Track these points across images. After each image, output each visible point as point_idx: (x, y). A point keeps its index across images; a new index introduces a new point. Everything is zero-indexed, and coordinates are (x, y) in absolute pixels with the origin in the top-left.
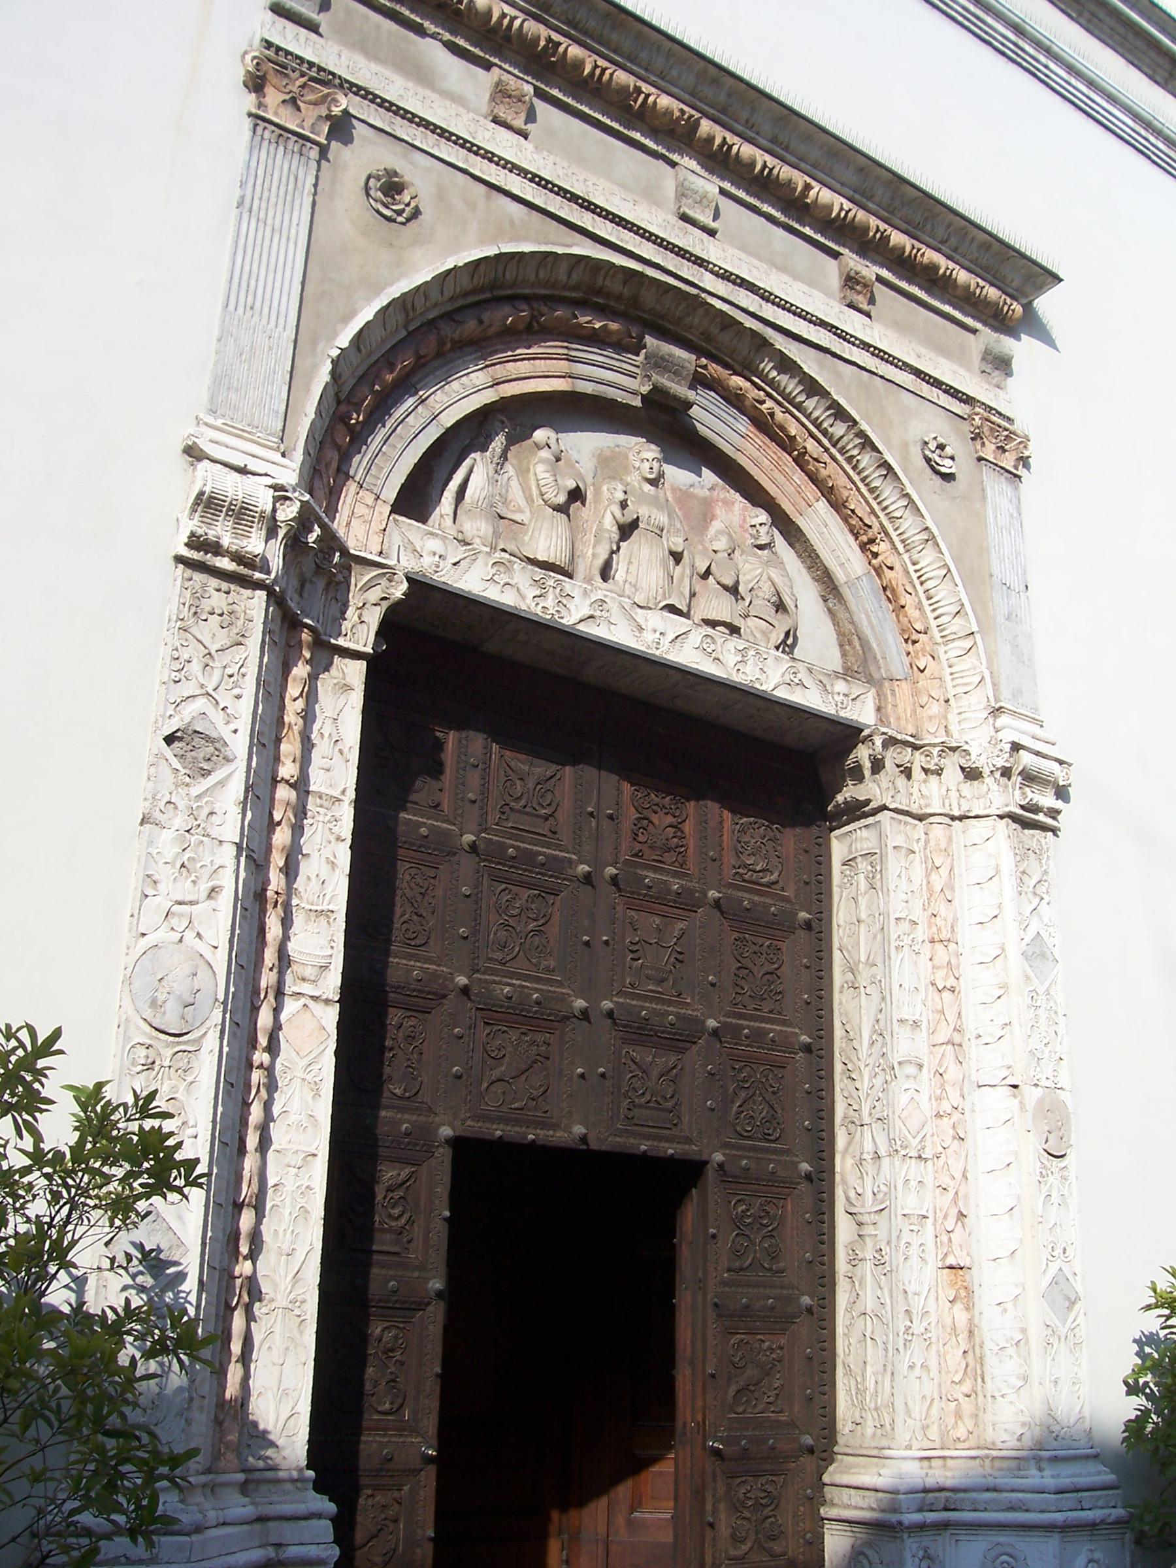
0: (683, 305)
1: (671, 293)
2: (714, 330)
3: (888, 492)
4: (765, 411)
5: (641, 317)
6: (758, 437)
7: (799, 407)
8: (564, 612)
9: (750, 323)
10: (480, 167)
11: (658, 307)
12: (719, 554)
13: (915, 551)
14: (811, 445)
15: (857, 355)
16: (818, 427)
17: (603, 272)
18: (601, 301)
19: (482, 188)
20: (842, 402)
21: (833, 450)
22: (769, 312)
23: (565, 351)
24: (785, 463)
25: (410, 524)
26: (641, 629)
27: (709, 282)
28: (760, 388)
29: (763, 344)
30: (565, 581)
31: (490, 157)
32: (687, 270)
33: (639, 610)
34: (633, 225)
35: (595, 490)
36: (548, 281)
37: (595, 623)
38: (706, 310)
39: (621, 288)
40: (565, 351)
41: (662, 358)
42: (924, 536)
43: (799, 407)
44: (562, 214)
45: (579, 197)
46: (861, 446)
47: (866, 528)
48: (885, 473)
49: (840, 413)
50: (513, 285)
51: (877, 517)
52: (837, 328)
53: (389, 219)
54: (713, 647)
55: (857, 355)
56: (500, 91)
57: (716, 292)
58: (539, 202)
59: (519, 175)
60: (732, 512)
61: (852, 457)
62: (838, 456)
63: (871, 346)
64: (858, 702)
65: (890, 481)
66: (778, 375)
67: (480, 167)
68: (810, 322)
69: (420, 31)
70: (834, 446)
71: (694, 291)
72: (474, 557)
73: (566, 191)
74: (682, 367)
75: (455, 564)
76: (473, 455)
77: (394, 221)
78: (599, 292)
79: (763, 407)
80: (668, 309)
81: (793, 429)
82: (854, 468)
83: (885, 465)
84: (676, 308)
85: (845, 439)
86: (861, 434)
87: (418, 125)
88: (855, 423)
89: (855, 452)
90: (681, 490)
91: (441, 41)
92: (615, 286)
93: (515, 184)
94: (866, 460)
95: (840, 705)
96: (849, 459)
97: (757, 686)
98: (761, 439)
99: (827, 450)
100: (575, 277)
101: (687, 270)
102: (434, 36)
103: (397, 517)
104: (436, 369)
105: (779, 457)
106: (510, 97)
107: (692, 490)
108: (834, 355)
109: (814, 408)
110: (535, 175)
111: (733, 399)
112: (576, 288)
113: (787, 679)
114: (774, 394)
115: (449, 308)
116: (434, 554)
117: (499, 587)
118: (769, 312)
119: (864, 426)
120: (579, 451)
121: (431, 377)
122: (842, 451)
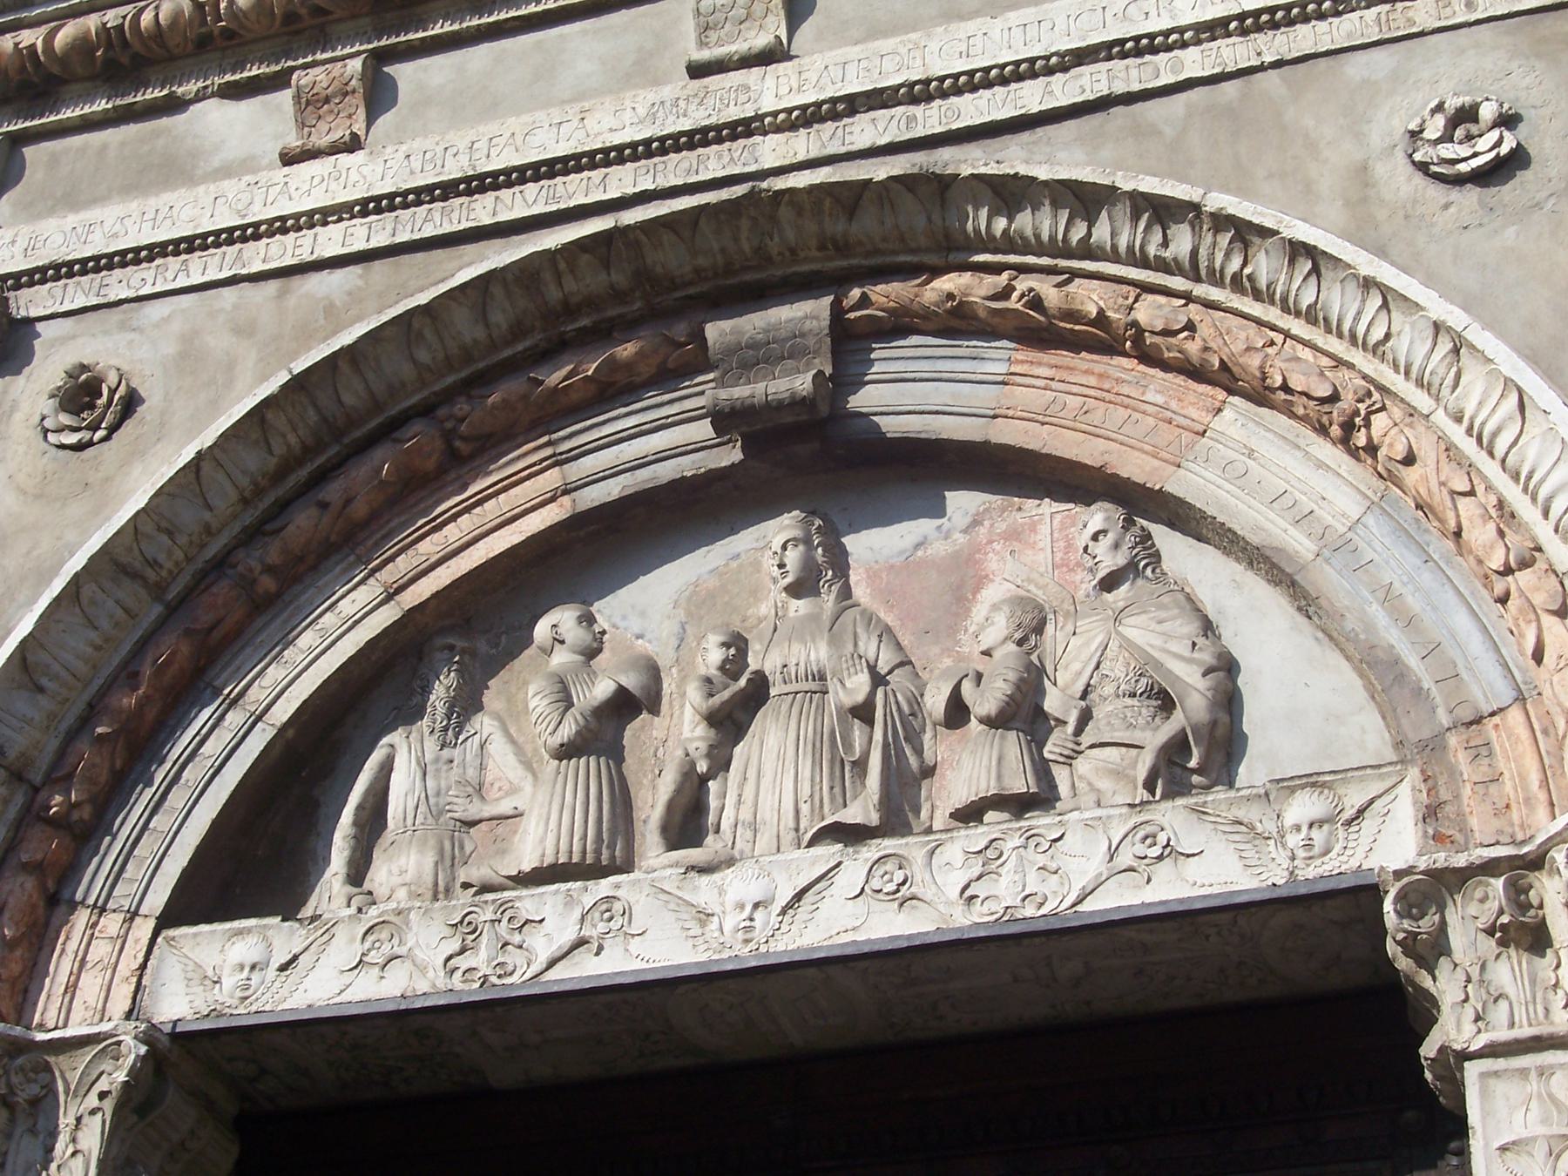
0: (745, 224)
1: (703, 222)
2: (838, 227)
3: (1339, 300)
4: (1019, 306)
5: (690, 297)
6: (1040, 364)
7: (1087, 251)
8: (513, 957)
9: (880, 170)
10: (259, 257)
11: (702, 261)
12: (997, 654)
13: (1445, 391)
14: (1149, 313)
15: (1194, 62)
16: (1144, 263)
17: (547, 276)
18: (585, 322)
19: (272, 286)
20: (1150, 185)
21: (1200, 290)
22: (932, 118)
23: (548, 451)
24: (1118, 381)
25: (195, 935)
26: (704, 916)
27: (770, 151)
28: (996, 269)
29: (942, 186)
30: (519, 898)
31: (281, 226)
32: (714, 162)
33: (705, 880)
34: (577, 157)
35: (680, 671)
36: (447, 358)
37: (589, 951)
38: (791, 203)
39: (603, 276)
40: (548, 451)
41: (750, 346)
42: (1445, 346)
43: (1087, 251)
44: (428, 232)
45: (457, 182)
46: (1238, 245)
47: (1326, 408)
48: (1309, 265)
49: (1163, 211)
50: (377, 406)
51: (1351, 366)
52: (1122, 42)
53: (79, 447)
54: (899, 876)
55: (1194, 62)
56: (308, 103)
57: (787, 162)
58: (380, 240)
59: (340, 220)
60: (1033, 546)
61: (1237, 278)
62: (1215, 294)
63: (1227, 20)
64: (1369, 824)
65: (1331, 274)
66: (1011, 219)
67: (259, 257)
68: (1050, 71)
69: (174, 105)
70: (1197, 279)
71: (739, 190)
72: (326, 937)
73: (430, 189)
74: (803, 335)
75: (283, 968)
76: (385, 740)
77: (90, 444)
78: (569, 310)
79: (1013, 303)
80: (723, 250)
81: (1090, 297)
82: (1257, 295)
83: (1298, 250)
84: (736, 240)
85: (1203, 253)
86: (1222, 221)
87: (150, 259)
88: (1195, 207)
89: (1235, 264)
90: (892, 567)
91: (213, 95)
92: (593, 280)
93: (331, 240)
94: (1265, 265)
95: (1301, 853)
96: (1237, 283)
97: (1029, 911)
98: (1045, 363)
99: (1188, 298)
100: (500, 318)
101: (714, 162)
102: (200, 97)
103: (171, 932)
104: (259, 631)
105: (1101, 376)
106: (327, 100)
107: (920, 553)
108: (1129, 99)
109: (1113, 234)
110: (364, 202)
111: (956, 323)
112: (518, 330)
113: (1125, 858)
114: (1031, 260)
115: (249, 518)
116: (242, 967)
117: (376, 971)
118: (932, 118)
119: (1218, 201)
120: (643, 614)
121: (248, 651)
122: (1216, 278)
